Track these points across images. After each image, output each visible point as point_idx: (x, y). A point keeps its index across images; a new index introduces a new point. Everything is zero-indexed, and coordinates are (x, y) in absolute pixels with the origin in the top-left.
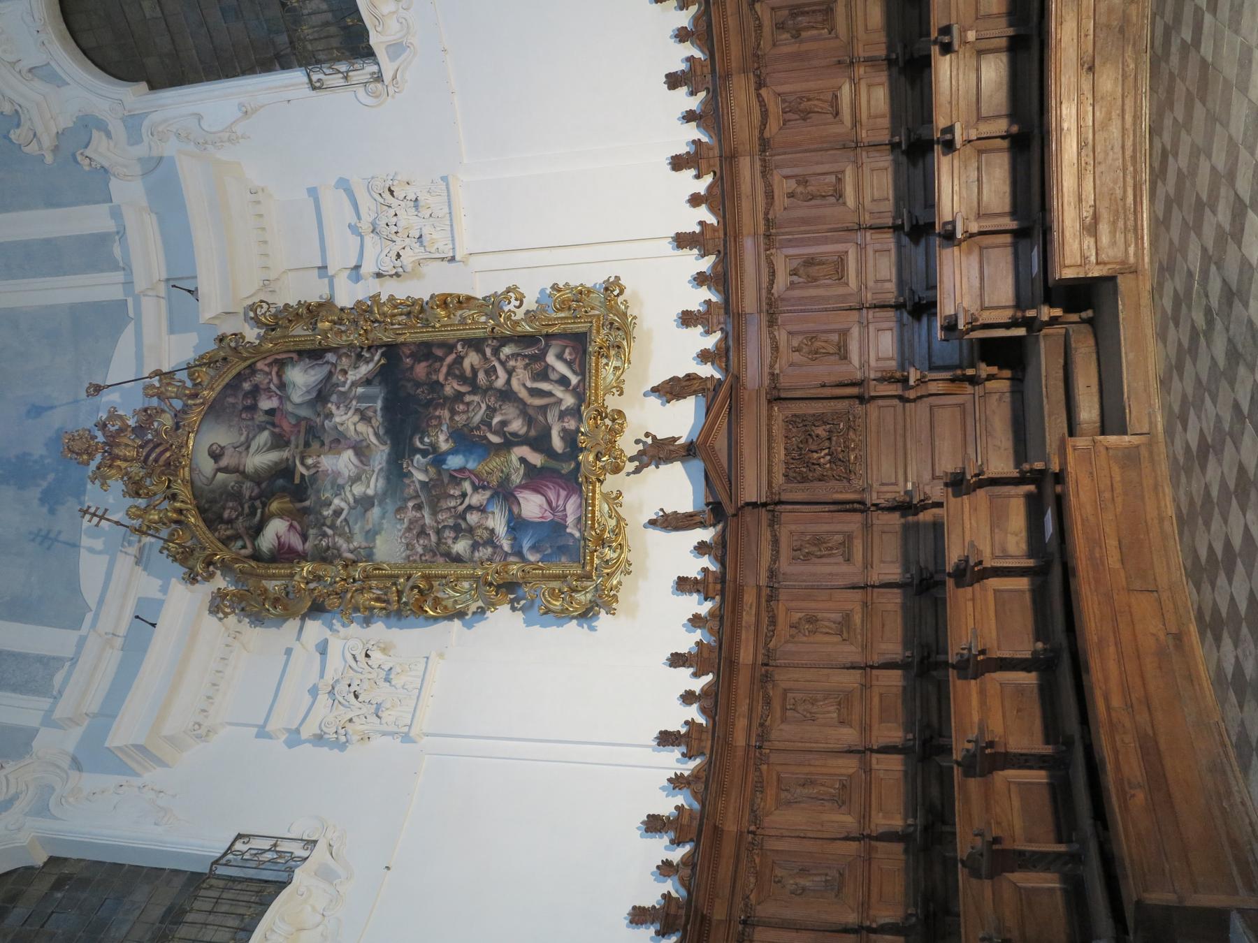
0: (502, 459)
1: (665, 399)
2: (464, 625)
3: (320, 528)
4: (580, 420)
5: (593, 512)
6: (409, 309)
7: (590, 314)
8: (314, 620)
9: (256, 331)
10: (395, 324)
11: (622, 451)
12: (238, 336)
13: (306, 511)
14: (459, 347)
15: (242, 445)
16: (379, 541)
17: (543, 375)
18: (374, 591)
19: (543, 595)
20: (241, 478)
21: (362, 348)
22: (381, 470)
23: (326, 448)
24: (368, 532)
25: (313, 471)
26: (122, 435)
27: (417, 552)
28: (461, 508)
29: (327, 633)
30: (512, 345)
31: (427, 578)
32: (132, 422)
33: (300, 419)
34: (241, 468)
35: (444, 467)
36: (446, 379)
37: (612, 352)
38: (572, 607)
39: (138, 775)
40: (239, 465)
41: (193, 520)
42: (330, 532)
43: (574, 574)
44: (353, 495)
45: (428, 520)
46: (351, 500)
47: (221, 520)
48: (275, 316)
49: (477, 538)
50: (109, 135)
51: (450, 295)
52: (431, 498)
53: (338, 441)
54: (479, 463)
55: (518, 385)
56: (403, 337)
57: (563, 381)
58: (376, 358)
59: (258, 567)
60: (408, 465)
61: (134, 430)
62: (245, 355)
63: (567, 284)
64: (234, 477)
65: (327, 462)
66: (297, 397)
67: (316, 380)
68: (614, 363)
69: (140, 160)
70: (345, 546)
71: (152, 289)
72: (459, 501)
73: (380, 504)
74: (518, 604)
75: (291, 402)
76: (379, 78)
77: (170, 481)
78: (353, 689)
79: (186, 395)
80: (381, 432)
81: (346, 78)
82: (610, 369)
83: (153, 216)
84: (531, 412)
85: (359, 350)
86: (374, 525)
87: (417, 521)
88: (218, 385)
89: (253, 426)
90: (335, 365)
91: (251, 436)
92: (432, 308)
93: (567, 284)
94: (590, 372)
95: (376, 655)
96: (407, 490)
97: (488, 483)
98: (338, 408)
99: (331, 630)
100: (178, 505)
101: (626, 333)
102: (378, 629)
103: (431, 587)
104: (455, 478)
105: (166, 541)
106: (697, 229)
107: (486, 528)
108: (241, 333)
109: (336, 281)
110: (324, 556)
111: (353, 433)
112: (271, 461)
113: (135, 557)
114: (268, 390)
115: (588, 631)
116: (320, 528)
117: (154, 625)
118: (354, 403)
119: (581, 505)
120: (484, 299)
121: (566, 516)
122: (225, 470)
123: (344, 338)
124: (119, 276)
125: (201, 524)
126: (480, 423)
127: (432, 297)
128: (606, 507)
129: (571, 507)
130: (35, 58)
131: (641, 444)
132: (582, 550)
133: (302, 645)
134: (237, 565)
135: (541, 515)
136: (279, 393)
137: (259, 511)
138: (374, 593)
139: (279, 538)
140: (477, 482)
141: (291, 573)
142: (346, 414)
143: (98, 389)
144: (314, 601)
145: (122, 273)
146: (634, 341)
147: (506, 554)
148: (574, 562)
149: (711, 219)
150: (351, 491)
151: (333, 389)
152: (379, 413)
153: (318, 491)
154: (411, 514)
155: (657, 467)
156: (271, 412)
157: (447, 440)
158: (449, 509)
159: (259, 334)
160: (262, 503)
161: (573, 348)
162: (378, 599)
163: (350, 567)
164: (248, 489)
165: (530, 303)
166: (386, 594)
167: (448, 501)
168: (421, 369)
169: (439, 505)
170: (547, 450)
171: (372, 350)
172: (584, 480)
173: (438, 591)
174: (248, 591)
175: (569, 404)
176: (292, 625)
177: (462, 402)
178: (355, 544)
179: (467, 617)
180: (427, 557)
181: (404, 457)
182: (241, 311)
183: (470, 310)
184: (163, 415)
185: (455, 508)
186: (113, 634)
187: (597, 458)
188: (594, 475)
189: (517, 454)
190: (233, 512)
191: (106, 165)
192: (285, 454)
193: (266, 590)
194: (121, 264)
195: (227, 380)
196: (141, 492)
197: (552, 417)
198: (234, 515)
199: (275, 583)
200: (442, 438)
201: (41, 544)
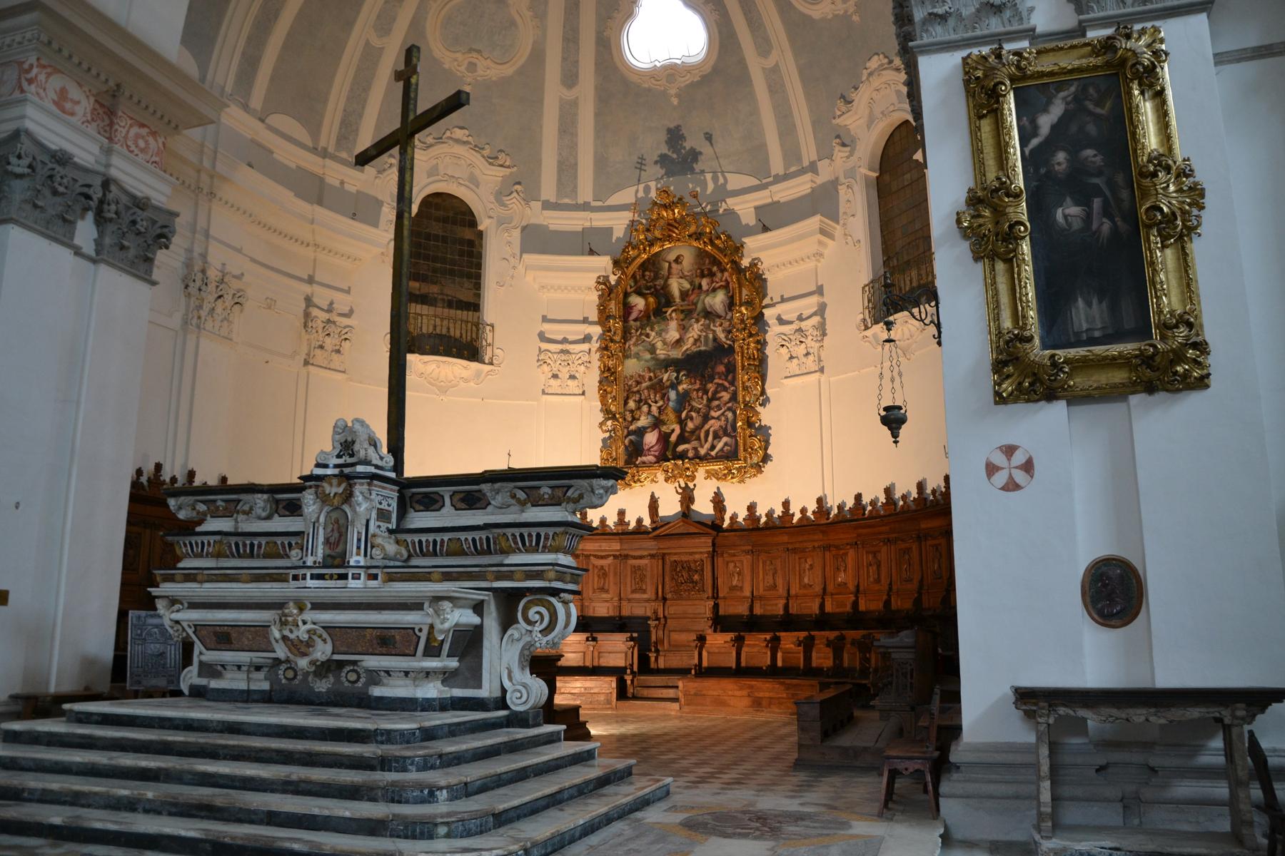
13: (648, 317)
17: (717, 436)
20: (665, 277)
22: (669, 355)
23: (681, 323)
24: (638, 354)
25: (669, 317)
28: (650, 402)
29: (595, 338)
33: (695, 304)
42: (638, 333)
45: (644, 385)
46: (654, 342)
47: (644, 272)
50: (848, 157)
57: (713, 447)
58: (728, 342)
64: (666, 273)
65: (673, 325)
66: (708, 300)
69: (837, 179)
70: (632, 342)
76: (867, 328)
80: (688, 352)
83: (809, 191)
84: (697, 432)
90: (725, 318)
95: (582, 368)
102: (596, 364)
104: (664, 396)
106: (791, 512)
114: (712, 282)
122: (670, 267)
129: (651, 458)
149: (795, 520)
152: (698, 349)
153: (658, 323)
154: (647, 376)
156: (700, 286)
161: (730, 451)
164: (660, 282)
168: (721, 368)
170: (678, 443)
181: (675, 367)
192: (678, 300)
197: (695, 443)
198: (647, 278)
200: (685, 386)
201: (638, 163)
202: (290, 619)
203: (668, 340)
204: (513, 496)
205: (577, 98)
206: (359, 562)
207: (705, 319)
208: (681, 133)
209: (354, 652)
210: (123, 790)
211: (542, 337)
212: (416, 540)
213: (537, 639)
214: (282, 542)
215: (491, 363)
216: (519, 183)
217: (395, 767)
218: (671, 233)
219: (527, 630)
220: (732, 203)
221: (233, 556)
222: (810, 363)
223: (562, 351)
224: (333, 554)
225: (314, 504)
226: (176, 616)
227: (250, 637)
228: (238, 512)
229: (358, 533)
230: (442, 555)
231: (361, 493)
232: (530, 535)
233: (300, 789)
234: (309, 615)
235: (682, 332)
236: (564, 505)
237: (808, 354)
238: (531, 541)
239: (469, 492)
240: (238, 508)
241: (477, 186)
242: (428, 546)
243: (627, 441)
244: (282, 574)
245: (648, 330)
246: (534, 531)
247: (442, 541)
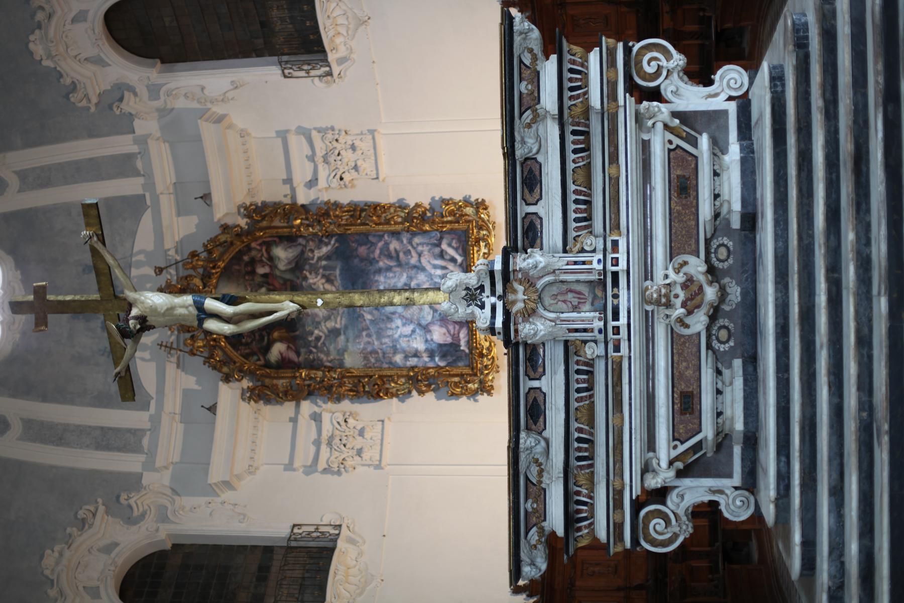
2: (399, 401)
5: (476, 338)
19: (451, 385)
29: (317, 409)
36: (379, 257)
39: (218, 496)
42: (314, 350)
44: (327, 328)
46: (326, 331)
47: (242, 344)
50: (135, 94)
58: (333, 242)
66: (282, 266)
70: (325, 359)
73: (345, 334)
75: (278, 269)
76: (330, 74)
78: (344, 442)
81: (308, 73)
83: (167, 145)
90: (305, 246)
95: (351, 421)
98: (311, 274)
102: (346, 405)
110: (313, 365)
114: (261, 261)
118: (321, 271)
124: (141, 180)
130: (91, 52)
134: (258, 372)
137: (266, 338)
139: (281, 354)
142: (316, 277)
150: (325, 326)
152: (338, 277)
153: (304, 326)
154: (366, 339)
156: (265, 276)
158: (389, 336)
159: (247, 222)
160: (267, 332)
162: (351, 390)
166: (356, 387)
168: (362, 250)
178: (332, 357)
186: (175, 413)
191: (134, 112)
194: (142, 173)
198: (249, 340)
202: (663, 291)
204: (529, 126)
205: (21, 419)
206: (599, 261)
207: (303, 270)
209: (695, 232)
210: (850, 273)
211: (311, 469)
212: (575, 225)
213: (676, 63)
214: (576, 400)
215: (340, 526)
216: (118, 497)
217: (804, 32)
219: (666, 78)
220: (169, 244)
221: (592, 466)
222: (364, 145)
223: (329, 444)
224: (590, 300)
225: (534, 324)
226: (664, 464)
227: (684, 364)
228: (540, 482)
229: (568, 264)
230: (590, 195)
231: (524, 260)
232: (571, 80)
233: (832, 98)
234: (659, 273)
236: (538, 68)
237: (353, 148)
238: (576, 79)
239: (524, 182)
240: (535, 481)
241: (116, 544)
242: (581, 211)
244: (613, 369)
246: (567, 75)
247: (576, 192)
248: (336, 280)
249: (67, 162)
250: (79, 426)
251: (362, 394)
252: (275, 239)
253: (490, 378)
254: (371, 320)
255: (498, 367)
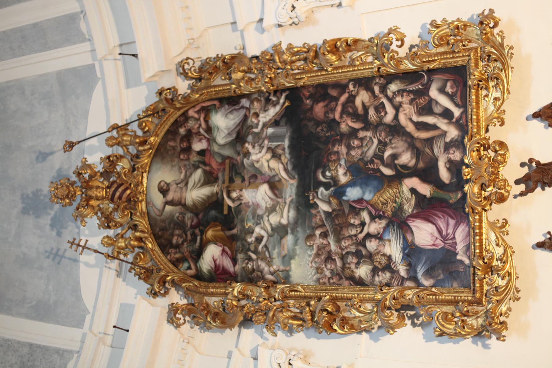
0: (395, 190)
1: (547, 123)
2: (371, 338)
3: (246, 253)
4: (464, 152)
5: (481, 241)
6: (305, 55)
7: (467, 47)
8: (248, 329)
9: (188, 83)
10: (295, 70)
11: (505, 181)
12: (173, 90)
13: (233, 238)
14: (351, 87)
15: (182, 181)
16: (294, 264)
18: (292, 309)
19: (438, 318)
20: (183, 209)
21: (270, 94)
22: (291, 201)
23: (247, 182)
24: (284, 257)
25: (237, 203)
26: (93, 179)
27: (326, 276)
28: (361, 236)
29: (261, 341)
30: (398, 82)
31: (334, 300)
32: (100, 168)
33: (224, 158)
34: (183, 201)
35: (344, 198)
36: (341, 117)
37: (492, 84)
38: (465, 331)
40: (181, 198)
41: (150, 245)
42: (254, 256)
43: (465, 300)
44: (271, 224)
45: (333, 247)
46: (269, 229)
48: (201, 70)
49: (377, 264)
51: (340, 39)
52: (335, 227)
53: (254, 176)
54: (375, 194)
55: (406, 119)
56: (303, 81)
57: (447, 114)
58: (282, 101)
59: (201, 285)
60: (314, 197)
61: (102, 174)
62: (178, 105)
63: (444, 20)
66: (221, 138)
67: (235, 123)
68: (495, 94)
70: (266, 269)
71: (110, 54)
72: (359, 230)
73: (293, 233)
74: (418, 320)
75: (217, 143)
77: (131, 214)
79: (137, 143)
80: (290, 167)
82: (490, 99)
84: (418, 145)
85: (267, 94)
86: (288, 251)
87: (324, 248)
88: (161, 132)
89: (189, 165)
90: (248, 109)
91: (188, 173)
92: (324, 54)
93: (444, 20)
94: (471, 105)
96: (314, 220)
97: (383, 212)
98: (254, 147)
99: (262, 338)
100: (138, 234)
101: (503, 64)
103: (338, 309)
105: (132, 263)
107: (384, 255)
108: (174, 87)
109: (246, 34)
111: (266, 169)
112: (205, 195)
113: (116, 271)
114: (199, 133)
115: (482, 349)
116: (246, 253)
117: (128, 331)
118: (266, 142)
119: (468, 234)
120: (370, 40)
121: (456, 243)
123: (254, 85)
124: (86, 46)
125: (157, 249)
126: (373, 157)
127: (325, 42)
128: (493, 237)
129: (460, 234)
131: (526, 167)
132: (472, 277)
133: (240, 351)
134: (184, 285)
135: (432, 243)
136: (207, 136)
137: (199, 238)
138: (292, 312)
139: (215, 261)
140: (373, 213)
141: (225, 292)
142: (260, 152)
143: (70, 145)
144: (245, 317)
145: (88, 43)
146: (512, 72)
147: (403, 278)
148: (465, 287)
150: (268, 220)
151: (248, 131)
152: (287, 150)
153: (242, 221)
154: (319, 241)
155: (543, 189)
156: (202, 153)
157: (345, 174)
158: (350, 237)
159: (189, 85)
160: (200, 230)
161: (453, 80)
162: (295, 318)
163: (271, 288)
165: (412, 38)
167: (350, 228)
168: (319, 109)
169: (342, 233)
171: (278, 94)
172: (471, 211)
173: (345, 311)
174: (193, 305)
175: (453, 136)
176: (231, 334)
177: (356, 137)
178: (275, 267)
179: (373, 331)
180: (334, 280)
181: (310, 190)
182: (173, 67)
183: (358, 51)
184: (122, 160)
185: (356, 235)
186: (105, 334)
187: (483, 187)
188: (480, 206)
189: (408, 185)
190: (179, 239)
192: (215, 189)
193: (208, 305)
194: (87, 37)
195: (167, 127)
196: (110, 225)
197: (438, 149)
199: (214, 299)
201: (54, 259)
203: (270, 203)
208: (31, 195)
218: (125, 196)
235: (259, 180)
243: (426, 283)
245: (251, 239)
248: (284, 153)
249: (11, 30)
250: (8, 340)
251: (310, 324)
252: (216, 102)
253: (504, 308)
254: (327, 213)
255: (518, 291)
